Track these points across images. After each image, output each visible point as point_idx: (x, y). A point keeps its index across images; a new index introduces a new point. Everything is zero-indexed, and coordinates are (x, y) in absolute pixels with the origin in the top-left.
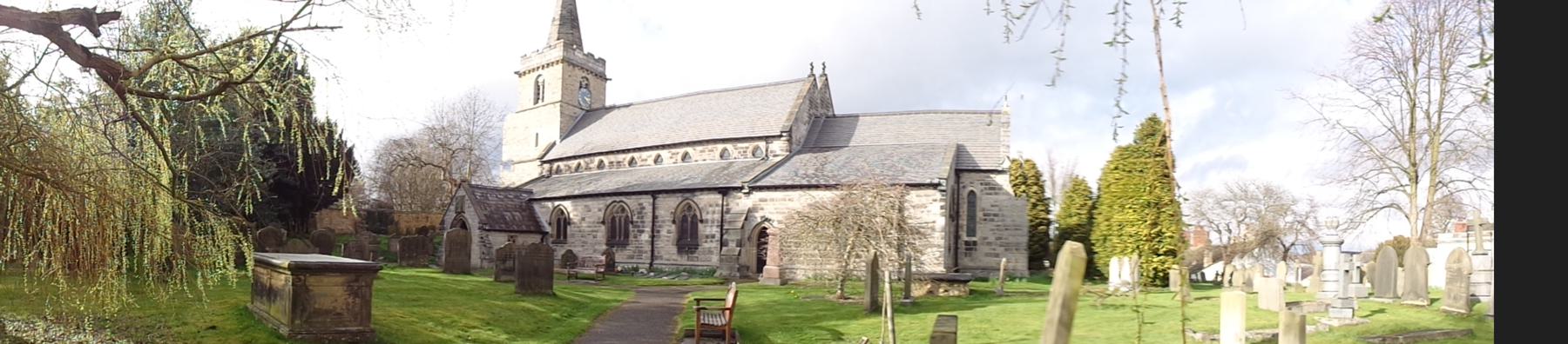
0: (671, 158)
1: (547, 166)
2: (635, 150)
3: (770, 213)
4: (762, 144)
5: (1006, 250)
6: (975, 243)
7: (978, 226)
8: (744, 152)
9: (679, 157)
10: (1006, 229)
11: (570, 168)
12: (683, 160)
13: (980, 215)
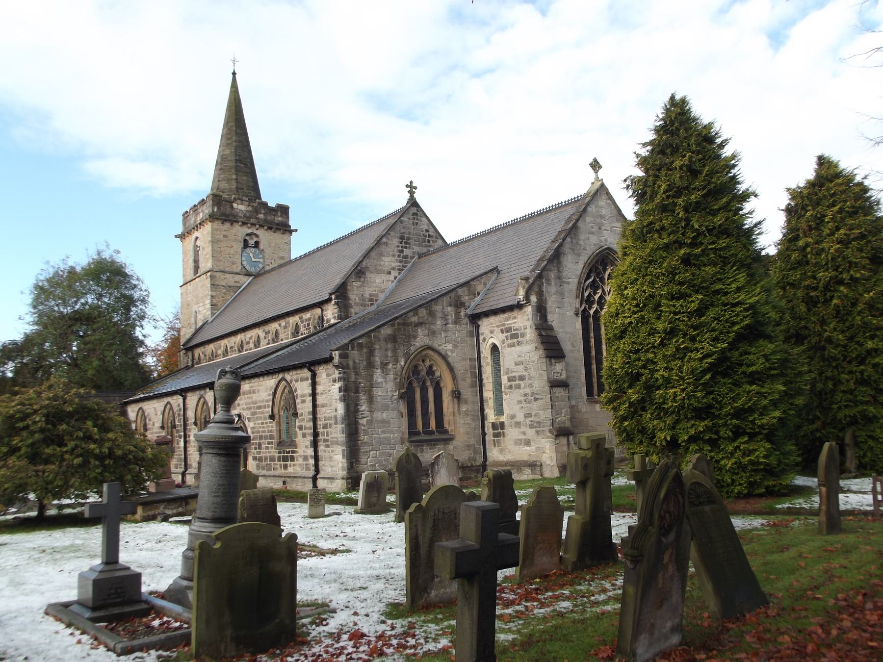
1: (190, 354)
3: (244, 409)
4: (318, 311)
5: (537, 432)
6: (502, 425)
7: (504, 397)
8: (308, 325)
10: (536, 399)
11: (205, 356)
12: (273, 340)
13: (504, 379)
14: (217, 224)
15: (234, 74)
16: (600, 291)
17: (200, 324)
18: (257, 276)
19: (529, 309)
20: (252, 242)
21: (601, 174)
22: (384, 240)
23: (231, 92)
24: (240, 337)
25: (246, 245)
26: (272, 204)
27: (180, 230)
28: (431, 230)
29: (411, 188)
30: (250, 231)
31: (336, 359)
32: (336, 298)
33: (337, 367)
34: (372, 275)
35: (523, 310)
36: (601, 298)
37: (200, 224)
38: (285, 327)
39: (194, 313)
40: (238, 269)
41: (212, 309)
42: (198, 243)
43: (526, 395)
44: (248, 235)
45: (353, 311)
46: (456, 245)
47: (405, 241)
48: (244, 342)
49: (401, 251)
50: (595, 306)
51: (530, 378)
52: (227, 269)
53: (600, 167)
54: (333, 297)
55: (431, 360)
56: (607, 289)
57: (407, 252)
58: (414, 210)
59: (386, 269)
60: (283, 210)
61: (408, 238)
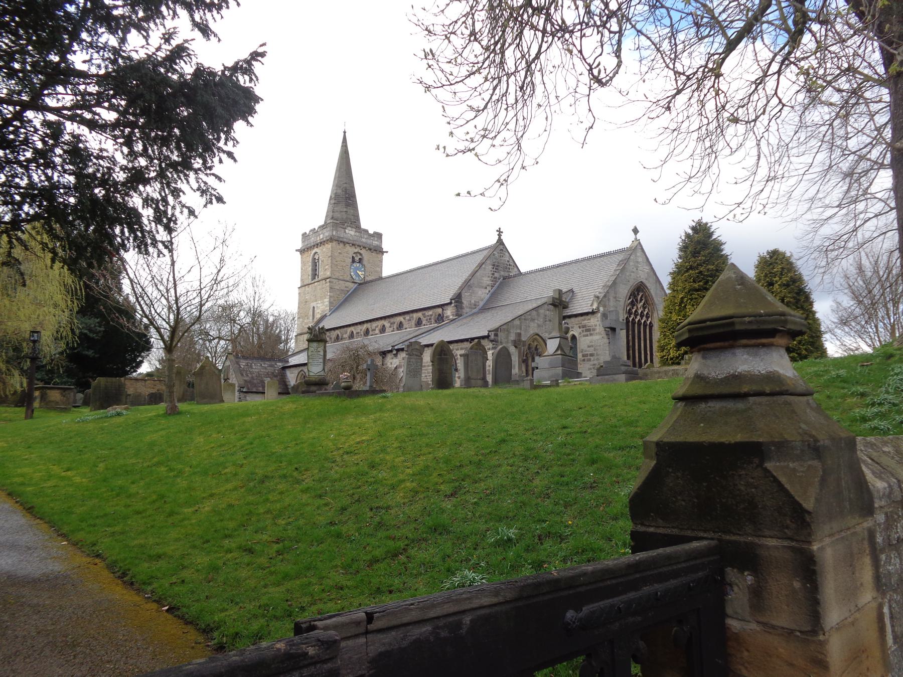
0: (390, 327)
2: (367, 322)
4: (440, 310)
9: (395, 327)
11: (331, 338)
14: (334, 243)
15: (345, 132)
16: (635, 307)
17: (318, 316)
18: (360, 284)
19: (599, 315)
20: (357, 259)
21: (639, 236)
22: (483, 266)
23: (342, 146)
24: (365, 326)
25: (353, 261)
26: (371, 232)
27: (299, 246)
28: (511, 261)
29: (500, 232)
30: (356, 251)
31: (492, 337)
32: (456, 302)
33: (492, 341)
34: (475, 289)
35: (595, 315)
36: (636, 311)
37: (321, 243)
38: (409, 320)
39: (312, 308)
40: (348, 278)
41: (330, 306)
42: (317, 257)
43: (594, 365)
44: (355, 253)
45: (464, 311)
46: (531, 272)
47: (496, 267)
48: (370, 330)
49: (493, 274)
50: (633, 316)
51: (597, 355)
52: (341, 278)
53: (638, 232)
54: (453, 301)
55: (538, 341)
56: (639, 306)
57: (496, 275)
58: (501, 247)
59: (485, 285)
60: (378, 236)
61: (497, 266)
